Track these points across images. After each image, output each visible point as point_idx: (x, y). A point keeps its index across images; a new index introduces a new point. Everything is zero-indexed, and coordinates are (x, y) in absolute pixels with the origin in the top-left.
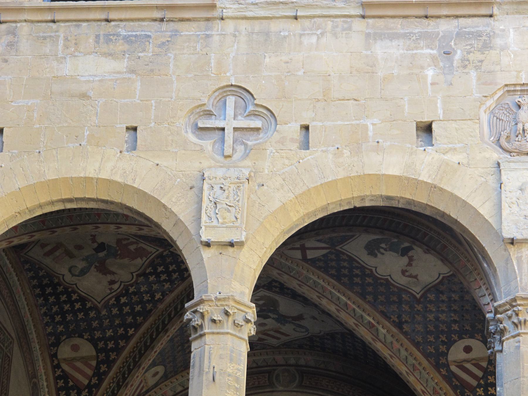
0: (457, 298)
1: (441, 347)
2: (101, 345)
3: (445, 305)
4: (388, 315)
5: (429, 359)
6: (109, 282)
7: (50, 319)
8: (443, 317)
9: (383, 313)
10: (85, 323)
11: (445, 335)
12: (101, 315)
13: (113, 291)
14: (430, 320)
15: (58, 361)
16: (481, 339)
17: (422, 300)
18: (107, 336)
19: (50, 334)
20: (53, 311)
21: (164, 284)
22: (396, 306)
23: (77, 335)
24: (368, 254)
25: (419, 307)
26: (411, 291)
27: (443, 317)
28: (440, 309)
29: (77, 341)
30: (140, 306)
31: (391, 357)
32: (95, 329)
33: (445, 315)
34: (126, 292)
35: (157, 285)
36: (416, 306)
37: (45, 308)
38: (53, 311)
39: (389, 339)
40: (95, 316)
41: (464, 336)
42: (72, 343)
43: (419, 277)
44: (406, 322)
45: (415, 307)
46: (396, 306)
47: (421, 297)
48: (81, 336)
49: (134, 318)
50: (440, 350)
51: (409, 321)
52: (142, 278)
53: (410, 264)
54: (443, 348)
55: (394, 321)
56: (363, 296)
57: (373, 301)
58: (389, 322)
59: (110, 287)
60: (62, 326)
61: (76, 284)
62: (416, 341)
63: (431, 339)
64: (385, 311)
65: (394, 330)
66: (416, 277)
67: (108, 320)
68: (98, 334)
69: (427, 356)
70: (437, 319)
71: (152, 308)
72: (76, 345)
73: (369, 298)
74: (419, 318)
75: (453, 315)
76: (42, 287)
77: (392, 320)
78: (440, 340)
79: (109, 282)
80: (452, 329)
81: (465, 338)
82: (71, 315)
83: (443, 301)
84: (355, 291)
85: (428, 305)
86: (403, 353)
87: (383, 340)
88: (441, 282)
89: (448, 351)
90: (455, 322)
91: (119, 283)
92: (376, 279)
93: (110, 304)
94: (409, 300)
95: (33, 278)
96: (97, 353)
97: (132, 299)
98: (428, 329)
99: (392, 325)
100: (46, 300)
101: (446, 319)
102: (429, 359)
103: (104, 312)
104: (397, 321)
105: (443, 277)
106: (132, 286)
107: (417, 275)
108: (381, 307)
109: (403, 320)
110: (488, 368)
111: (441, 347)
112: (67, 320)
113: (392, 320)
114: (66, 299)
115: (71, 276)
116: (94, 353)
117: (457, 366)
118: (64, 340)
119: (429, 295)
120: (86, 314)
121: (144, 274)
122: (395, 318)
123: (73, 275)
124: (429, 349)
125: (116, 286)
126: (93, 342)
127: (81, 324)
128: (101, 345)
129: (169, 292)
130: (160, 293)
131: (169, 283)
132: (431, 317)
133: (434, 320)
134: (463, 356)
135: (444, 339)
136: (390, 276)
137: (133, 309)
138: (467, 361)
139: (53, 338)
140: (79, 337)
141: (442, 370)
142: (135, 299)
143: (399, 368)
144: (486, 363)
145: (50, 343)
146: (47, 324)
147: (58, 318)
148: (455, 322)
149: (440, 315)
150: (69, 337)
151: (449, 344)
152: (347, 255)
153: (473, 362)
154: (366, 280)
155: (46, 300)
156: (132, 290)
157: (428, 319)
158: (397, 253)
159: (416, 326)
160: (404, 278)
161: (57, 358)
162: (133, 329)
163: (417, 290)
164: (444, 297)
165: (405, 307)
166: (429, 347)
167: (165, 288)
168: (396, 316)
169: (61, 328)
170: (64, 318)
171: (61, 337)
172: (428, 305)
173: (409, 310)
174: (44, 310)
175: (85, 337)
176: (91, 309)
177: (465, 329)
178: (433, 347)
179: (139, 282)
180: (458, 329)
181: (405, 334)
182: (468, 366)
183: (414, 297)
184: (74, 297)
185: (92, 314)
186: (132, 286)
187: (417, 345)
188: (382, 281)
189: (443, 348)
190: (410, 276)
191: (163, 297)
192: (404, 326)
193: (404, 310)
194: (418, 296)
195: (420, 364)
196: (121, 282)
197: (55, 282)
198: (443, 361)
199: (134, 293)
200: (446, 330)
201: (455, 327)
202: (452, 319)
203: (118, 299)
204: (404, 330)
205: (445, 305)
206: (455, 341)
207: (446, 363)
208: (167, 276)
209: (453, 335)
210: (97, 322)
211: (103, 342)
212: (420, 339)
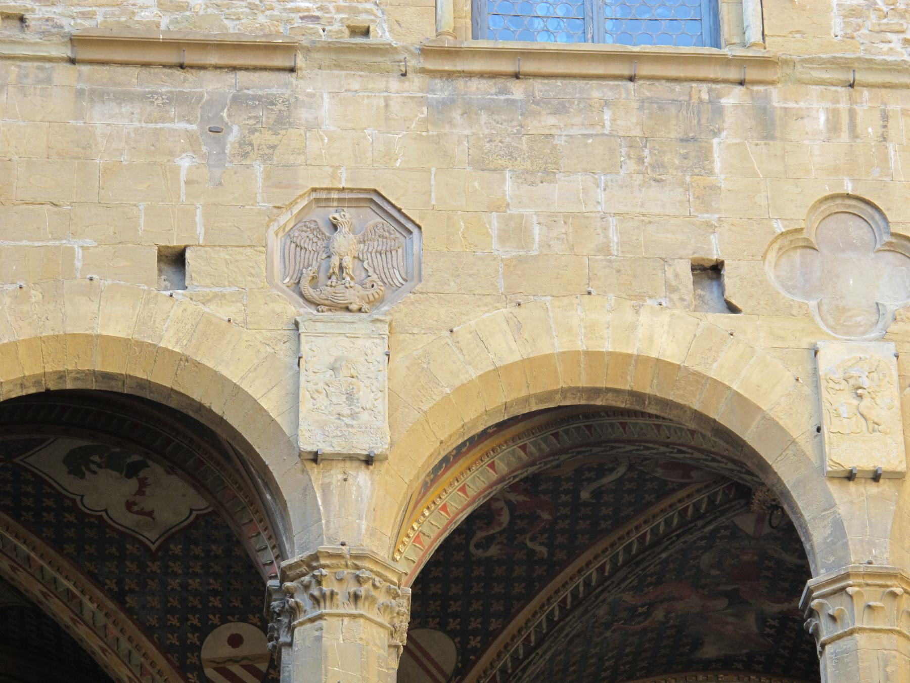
0: (220, 552)
1: (190, 635)
3: (200, 563)
5: (169, 656)
8: (195, 583)
9: (93, 577)
11: (197, 616)
14: (173, 589)
16: (259, 624)
17: (160, 554)
22: (116, 563)
24: (69, 473)
25: (155, 567)
26: (141, 538)
27: (195, 583)
28: (191, 571)
31: (104, 651)
33: (198, 580)
36: (149, 563)
39: (101, 619)
41: (230, 618)
43: (155, 515)
44: (132, 591)
45: (148, 566)
46: (116, 563)
47: (158, 549)
50: (189, 642)
51: (137, 589)
53: (140, 492)
54: (193, 638)
55: (110, 590)
56: (57, 544)
57: (75, 553)
62: (147, 624)
63: (174, 621)
64: (96, 571)
65: (110, 604)
66: (150, 514)
69: (165, 650)
70: (185, 586)
73: (70, 549)
74: (153, 585)
75: (211, 581)
77: (106, 587)
78: (189, 623)
80: (210, 605)
81: (231, 622)
83: (196, 557)
84: (44, 535)
85: (171, 564)
86: (125, 645)
87: (91, 622)
88: (194, 525)
89: (202, 643)
90: (215, 593)
94: (138, 554)
98: (169, 605)
99: (106, 596)
101: (200, 589)
102: (169, 656)
104: (116, 589)
105: (198, 517)
107: (153, 512)
108: (89, 565)
109: (127, 588)
110: (268, 673)
111: (190, 635)
113: (106, 587)
117: (216, 669)
119: (172, 546)
122: (111, 584)
124: (169, 639)
132: (175, 583)
133: (179, 589)
134: (226, 651)
135: (196, 622)
136: (106, 511)
138: (233, 660)
141: (190, 676)
143: (116, 670)
144: (267, 664)
148: (215, 593)
149: (190, 581)
151: (205, 631)
152: (34, 474)
153: (245, 662)
154: (64, 517)
157: (169, 588)
158: (121, 473)
159: (149, 598)
160: (130, 515)
163: (151, 537)
164: (198, 551)
165: (131, 566)
166: (169, 636)
168: (115, 580)
172: (171, 564)
173: (137, 571)
177: (231, 605)
178: (175, 635)
180: (220, 606)
181: (129, 612)
182: (235, 669)
183: (147, 548)
187: (148, 631)
188: (92, 520)
189: (193, 638)
190: (141, 512)
192: (128, 599)
193: (127, 570)
194: (153, 547)
195: (152, 664)
198: (192, 659)
200: (199, 606)
201: (216, 602)
202: (211, 587)
204: (128, 605)
205: (200, 563)
206: (214, 627)
207: (198, 663)
209: (211, 617)
212: (153, 621)
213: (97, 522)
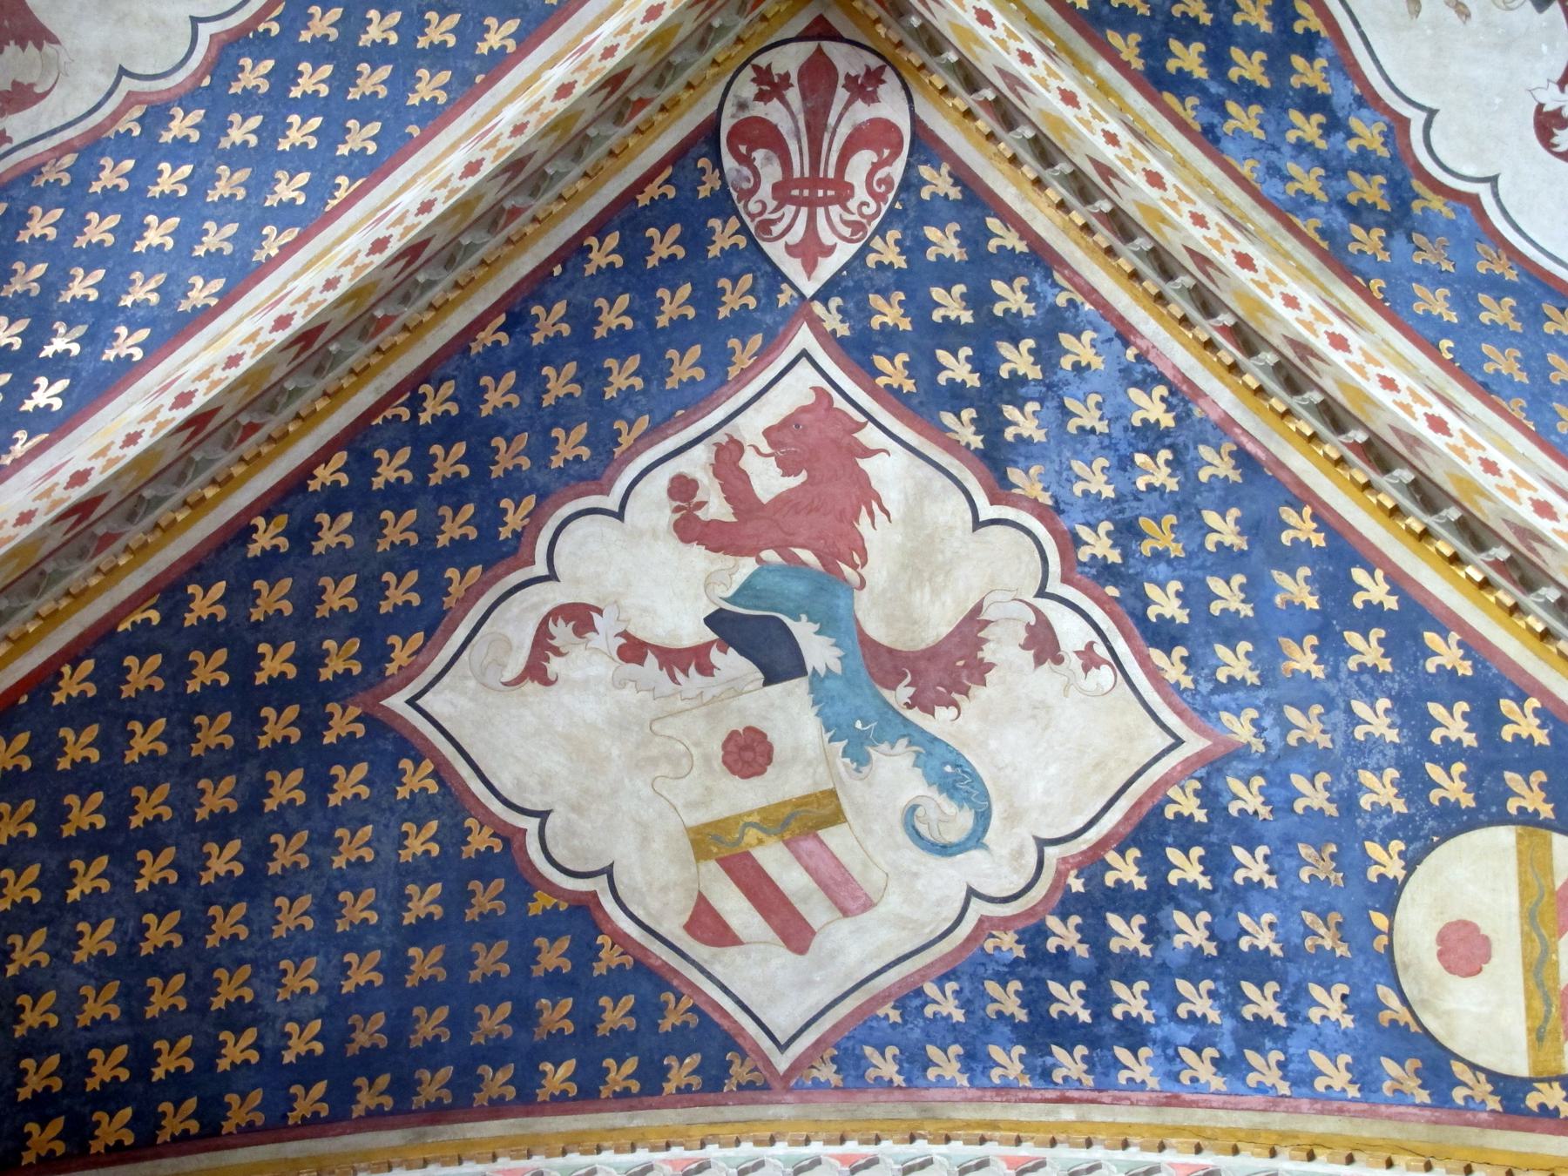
2: (1451, 786)
6: (1039, 661)
7: (1260, 1050)
10: (1305, 851)
12: (1258, 746)
13: (1100, 649)
15: (1549, 1080)
18: (1392, 736)
19: (1365, 1078)
20: (1214, 1016)
21: (1066, 363)
23: (1380, 920)
29: (1416, 927)
30: (1211, 518)
32: (1347, 800)
34: (1122, 583)
35: (1071, 404)
37: (1188, 1055)
38: (1214, 1016)
40: (1258, 781)
42: (1433, 965)
48: (1389, 895)
49: (1289, 559)
52: (1015, 475)
59: (1075, 663)
60: (1317, 991)
61: (1042, 844)
67: (1292, 714)
68: (1380, 790)
71: (1228, 447)
72: (1442, 938)
76: (1040, 1032)
79: (1039, 661)
82: (1244, 920)
91: (1046, 605)
93: (1187, 682)
95: (975, 1061)
96: (1503, 819)
97: (1159, 556)
100: (1134, 1034)
103: (1240, 728)
106: (1078, 542)
112: (1276, 950)
114: (1139, 919)
115: (976, 854)
116: (1505, 836)
118: (1404, 1000)
120: (1247, 831)
121: (995, 460)
123: (975, 839)
125: (1071, 632)
126: (1428, 828)
127: (1304, 875)
128: (1451, 786)
129: (1127, 344)
130: (1135, 394)
131: (1066, 339)
137: (1227, 560)
139: (1389, 1066)
140: (1390, 910)
142: (1162, 536)
145: (1423, 1096)
146: (1303, 1079)
147: (1263, 1003)
150: (1388, 969)
155: (1134, 1034)
156: (1099, 545)
161: (1526, 1085)
162: (1359, 575)
167: (1098, 363)
169: (1328, 1005)
170: (1260, 967)
171: (1384, 1018)
174: (1201, 1067)
175: (1395, 869)
176: (1210, 797)
179: (1046, 499)
184: (1126, 870)
185: (1247, 797)
186: (1070, 543)
191: (1160, 378)
196: (1042, 593)
197: (1019, 951)
199: (1127, 532)
203: (1162, 635)
208: (1015, 341)
210: (1299, 782)
211: (1434, 771)
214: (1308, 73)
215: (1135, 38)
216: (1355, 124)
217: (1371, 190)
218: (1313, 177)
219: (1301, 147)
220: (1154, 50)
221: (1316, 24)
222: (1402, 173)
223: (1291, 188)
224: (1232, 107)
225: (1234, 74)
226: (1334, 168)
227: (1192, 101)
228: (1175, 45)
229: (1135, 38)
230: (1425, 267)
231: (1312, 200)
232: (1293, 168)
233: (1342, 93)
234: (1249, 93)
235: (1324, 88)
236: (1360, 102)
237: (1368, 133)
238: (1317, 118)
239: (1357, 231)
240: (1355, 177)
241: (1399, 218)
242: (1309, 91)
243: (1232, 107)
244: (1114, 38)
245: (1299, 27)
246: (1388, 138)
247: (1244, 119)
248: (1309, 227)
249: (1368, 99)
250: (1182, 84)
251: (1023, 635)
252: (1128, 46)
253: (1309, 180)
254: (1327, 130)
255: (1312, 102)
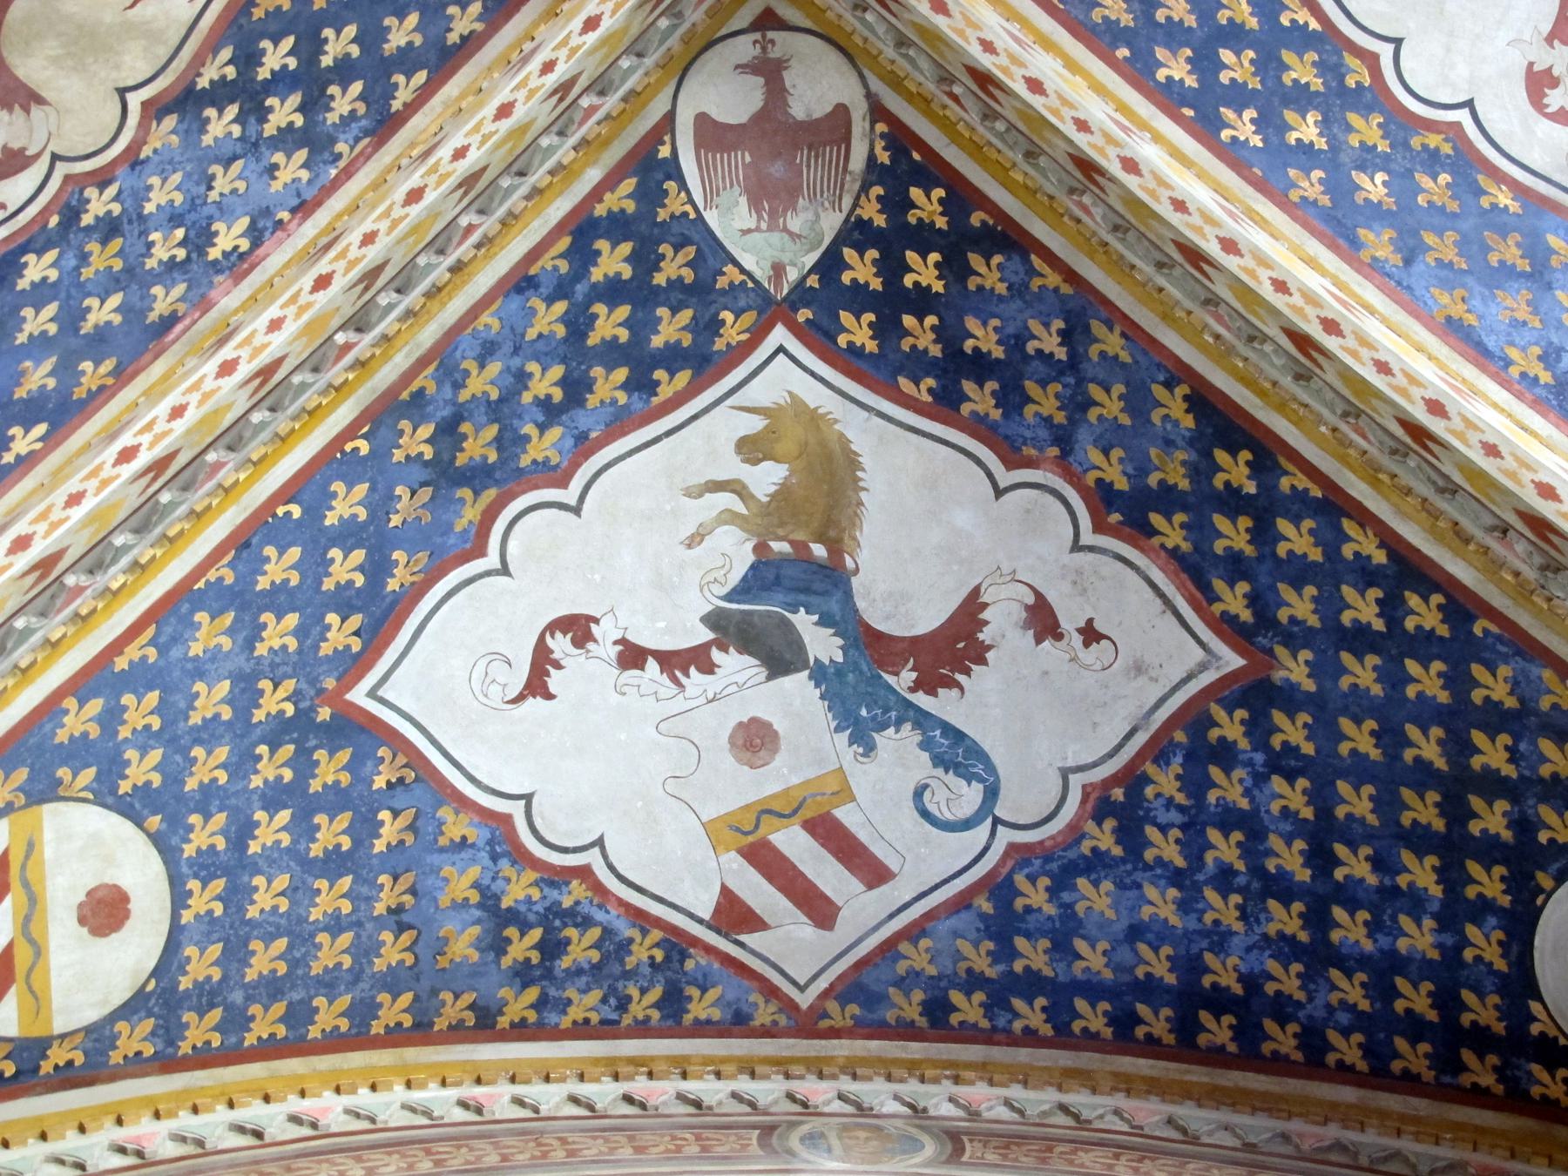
4: (1491, 342)
21: (279, 158)
30: (115, 300)
35: (238, 166)
49: (67, 370)
52: (170, 121)
57: (1397, 259)
58: (1505, 384)
64: (1471, 319)
71: (182, 308)
73: (1379, 243)
77: (1514, 372)
91: (45, 160)
92: (1400, 123)
97: (84, 258)
99: (1519, 396)
106: (103, 185)
108: (1445, 299)
113: (1514, 372)
121: (186, 102)
129: (293, 211)
130: (244, 222)
131: (302, 155)
136: (1469, 104)
142: (103, 258)
156: (99, 204)
160: (1545, 127)
167: (276, 186)
168: (1537, 350)
179: (146, 152)
186: (102, 179)
188: (1433, 140)
191: (257, 243)
196: (55, 158)
199: (109, 228)
213: (1447, 149)
214: (608, 385)
215: (630, 206)
216: (555, 433)
217: (478, 445)
218: (488, 388)
219: (522, 378)
220: (617, 227)
221: (665, 392)
222: (504, 476)
223: (470, 365)
224: (560, 307)
225: (600, 309)
226: (501, 409)
227: (564, 267)
228: (626, 248)
229: (630, 206)
230: (391, 498)
231: (458, 386)
232: (494, 368)
233: (589, 419)
234: (578, 324)
235: (592, 401)
236: (581, 438)
237: (545, 445)
238: (558, 395)
239: (426, 431)
240: (492, 431)
241: (446, 475)
242: (589, 386)
243: (560, 307)
244: (629, 185)
245: (660, 374)
246: (543, 466)
247: (548, 319)
248: (426, 380)
249: (584, 446)
250: (582, 255)
251: (16, 145)
252: (621, 199)
253: (482, 382)
254: (545, 403)
255: (576, 388)
